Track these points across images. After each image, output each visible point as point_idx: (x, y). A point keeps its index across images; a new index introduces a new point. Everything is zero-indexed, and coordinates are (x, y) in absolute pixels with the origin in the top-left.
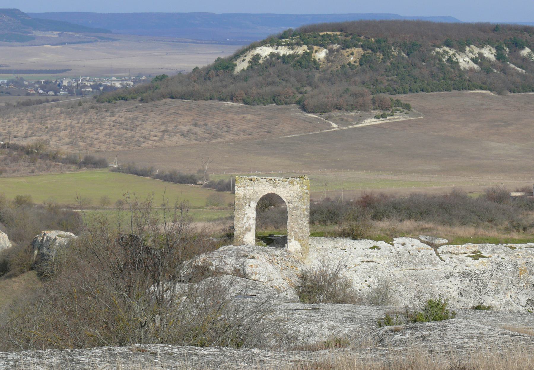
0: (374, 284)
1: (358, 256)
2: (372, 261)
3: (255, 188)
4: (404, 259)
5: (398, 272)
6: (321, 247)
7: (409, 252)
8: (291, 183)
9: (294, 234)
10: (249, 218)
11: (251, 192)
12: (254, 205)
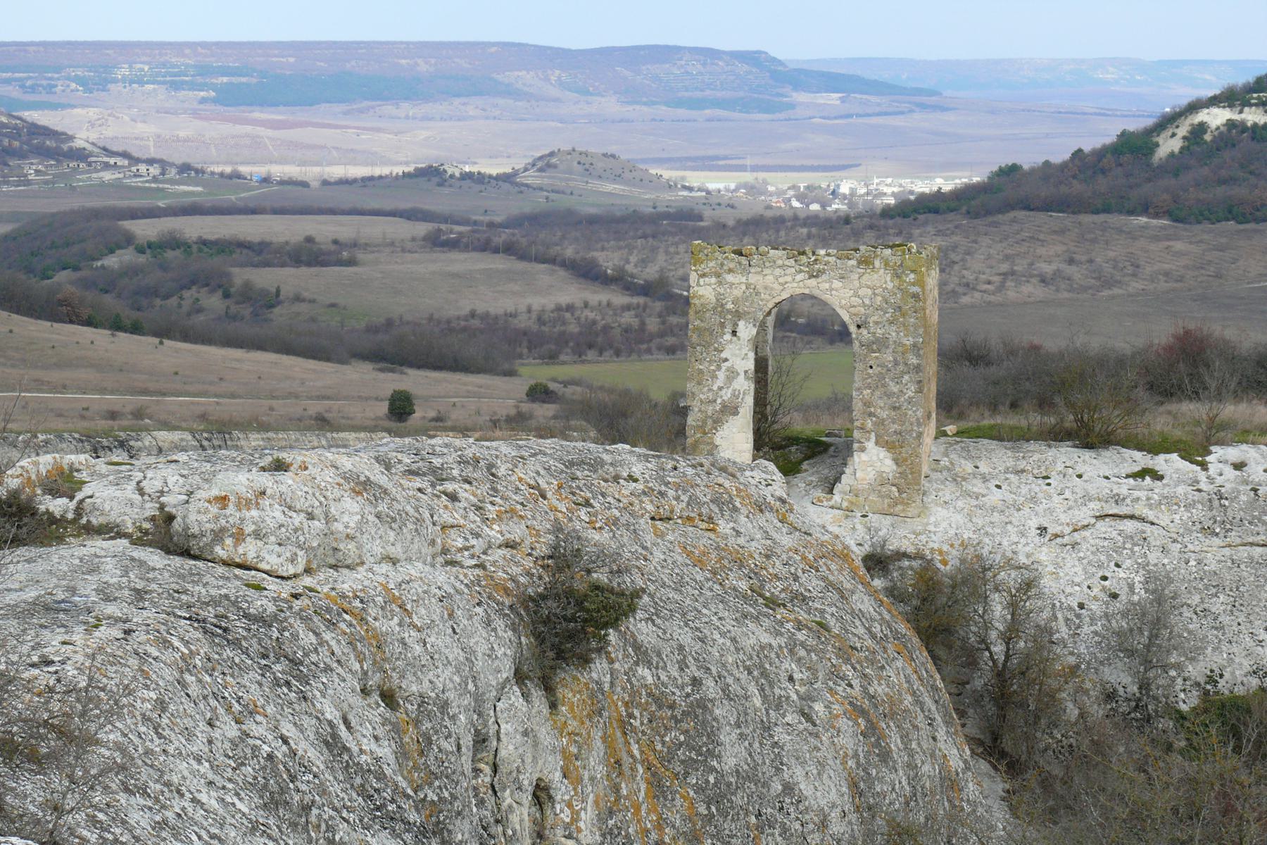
0: (1131, 587)
1: (1087, 498)
2: (1132, 517)
3: (753, 279)
4: (1235, 510)
5: (1214, 552)
6: (969, 467)
7: (1255, 490)
8: (866, 262)
9: (875, 424)
10: (732, 375)
11: (737, 293)
12: (747, 331)
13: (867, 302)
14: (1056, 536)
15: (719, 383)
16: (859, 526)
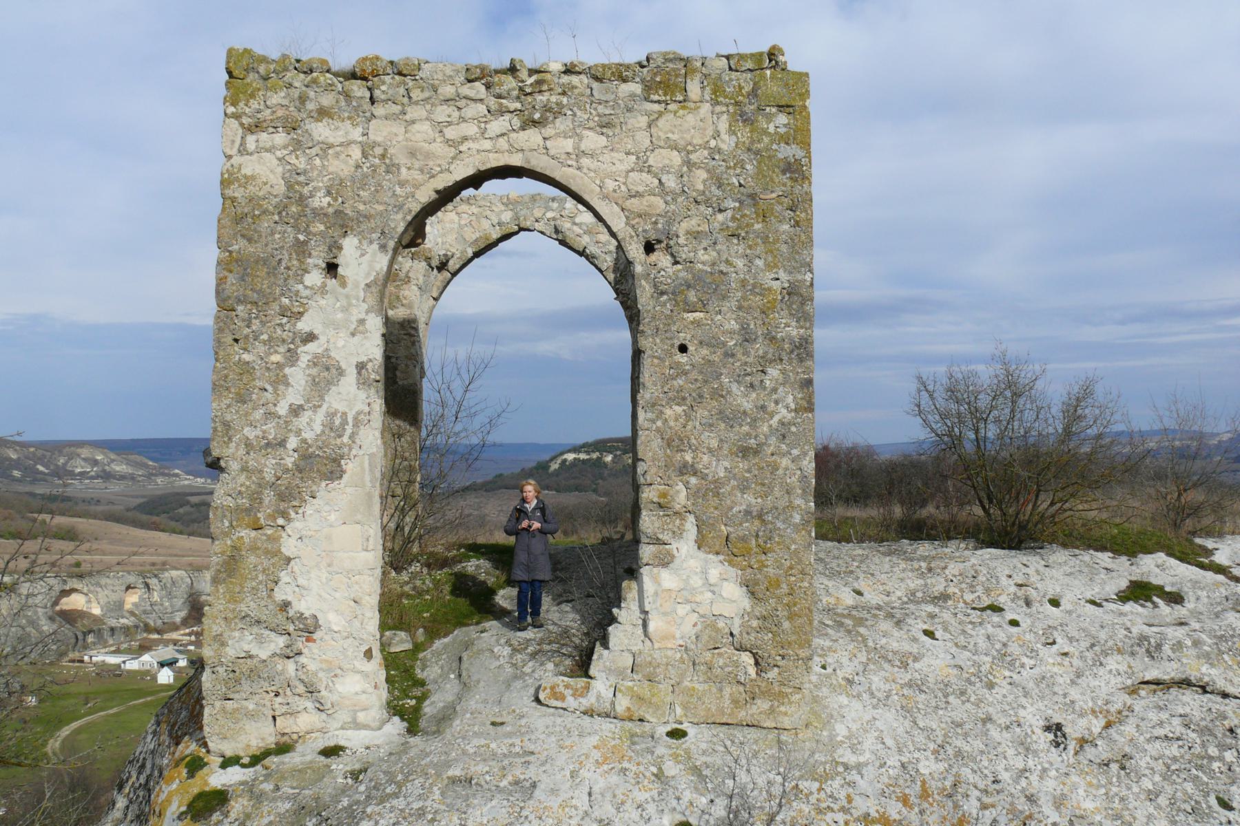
1: (1099, 651)
2: (1185, 683)
3: (381, 131)
6: (848, 599)
9: (694, 494)
10: (326, 373)
11: (341, 166)
13: (671, 182)
14: (1082, 742)
15: (293, 396)
16: (671, 769)
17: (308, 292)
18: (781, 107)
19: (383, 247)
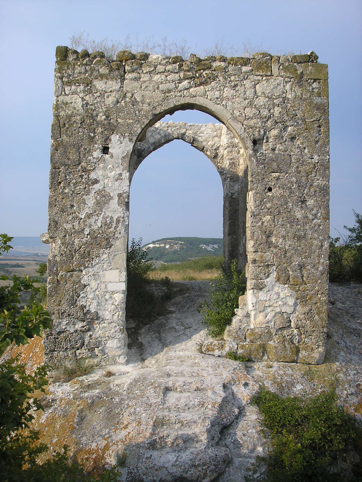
17: (95, 160)
18: (315, 80)
19: (131, 140)
